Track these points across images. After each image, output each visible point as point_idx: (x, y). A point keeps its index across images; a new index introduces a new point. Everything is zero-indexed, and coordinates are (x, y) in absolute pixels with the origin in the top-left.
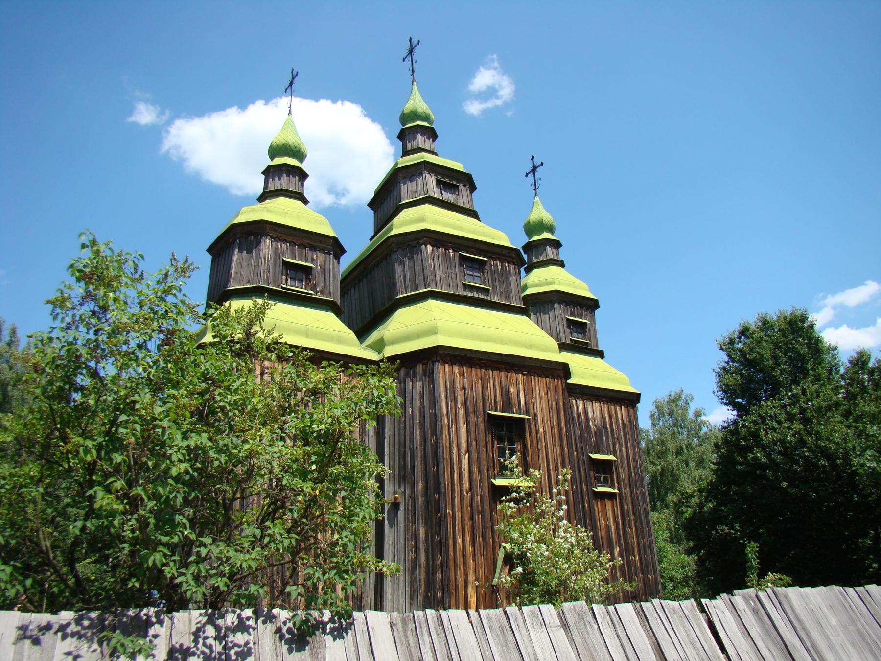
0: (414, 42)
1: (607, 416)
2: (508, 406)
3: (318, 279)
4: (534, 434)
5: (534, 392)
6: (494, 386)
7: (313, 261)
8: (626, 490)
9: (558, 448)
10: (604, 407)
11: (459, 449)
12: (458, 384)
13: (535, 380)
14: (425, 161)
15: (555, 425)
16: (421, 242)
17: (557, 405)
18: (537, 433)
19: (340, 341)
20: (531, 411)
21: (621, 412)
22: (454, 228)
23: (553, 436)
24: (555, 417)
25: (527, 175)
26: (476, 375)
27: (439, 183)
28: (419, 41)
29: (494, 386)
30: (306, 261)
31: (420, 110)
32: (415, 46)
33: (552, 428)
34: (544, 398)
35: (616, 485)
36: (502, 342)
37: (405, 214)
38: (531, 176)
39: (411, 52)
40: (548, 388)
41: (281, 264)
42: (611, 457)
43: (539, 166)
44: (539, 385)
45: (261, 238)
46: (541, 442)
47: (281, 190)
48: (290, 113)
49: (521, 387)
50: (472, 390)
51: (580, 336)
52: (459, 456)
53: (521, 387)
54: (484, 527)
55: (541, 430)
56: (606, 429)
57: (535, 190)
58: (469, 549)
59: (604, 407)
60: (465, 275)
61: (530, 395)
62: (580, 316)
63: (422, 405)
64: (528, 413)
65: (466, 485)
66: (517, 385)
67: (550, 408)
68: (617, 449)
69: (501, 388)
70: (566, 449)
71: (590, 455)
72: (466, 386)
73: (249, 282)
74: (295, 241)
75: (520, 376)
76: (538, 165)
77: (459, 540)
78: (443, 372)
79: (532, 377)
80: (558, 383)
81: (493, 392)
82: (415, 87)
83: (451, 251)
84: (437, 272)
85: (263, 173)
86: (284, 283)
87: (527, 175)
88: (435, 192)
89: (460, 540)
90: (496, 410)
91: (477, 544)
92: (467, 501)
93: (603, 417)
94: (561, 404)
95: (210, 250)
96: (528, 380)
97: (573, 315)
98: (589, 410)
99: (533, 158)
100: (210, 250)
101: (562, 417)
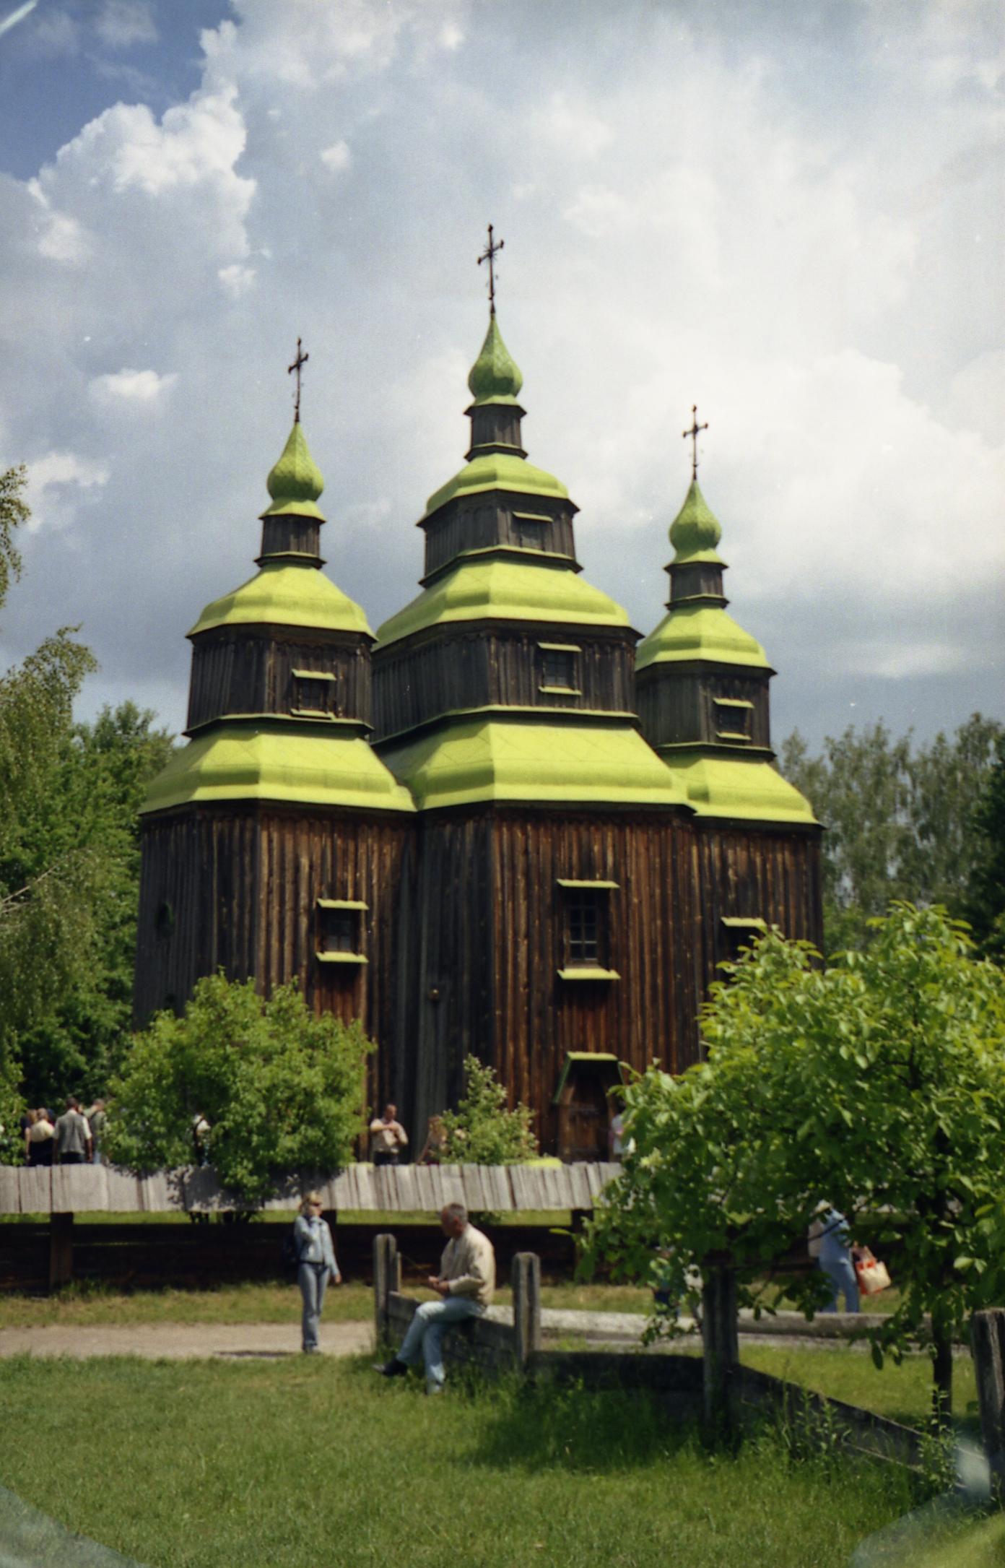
2: (586, 873)
5: (628, 847)
6: (570, 845)
7: (334, 670)
9: (659, 922)
11: (516, 934)
12: (519, 847)
15: (658, 891)
16: (482, 635)
17: (663, 864)
19: (368, 786)
20: (623, 875)
23: (652, 907)
24: (657, 881)
28: (502, 244)
29: (570, 845)
32: (497, 248)
36: (586, 781)
44: (637, 842)
48: (297, 420)
50: (538, 853)
52: (516, 944)
55: (635, 900)
58: (524, 1060)
61: (621, 853)
64: (616, 880)
65: (523, 978)
67: (650, 868)
68: (771, 909)
69: (580, 847)
70: (671, 923)
72: (530, 848)
77: (511, 1049)
83: (525, 641)
84: (502, 680)
90: (571, 878)
92: (523, 999)
93: (751, 863)
94: (669, 861)
97: (726, 695)
98: (730, 854)
101: (669, 880)
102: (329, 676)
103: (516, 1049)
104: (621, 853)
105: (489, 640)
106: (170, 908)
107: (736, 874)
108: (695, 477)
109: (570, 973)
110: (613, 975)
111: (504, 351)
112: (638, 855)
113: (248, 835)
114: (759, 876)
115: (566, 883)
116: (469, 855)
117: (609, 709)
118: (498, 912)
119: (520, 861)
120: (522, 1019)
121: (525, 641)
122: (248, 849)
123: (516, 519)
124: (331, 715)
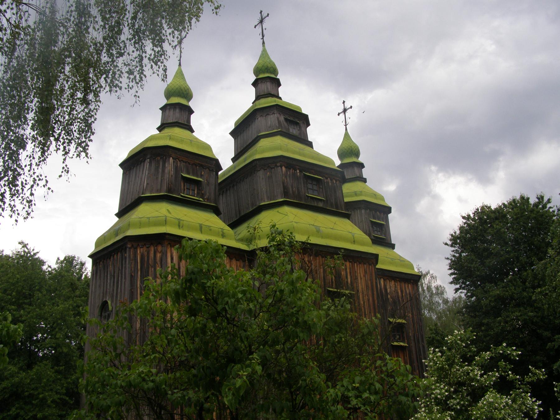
0: (264, 14)
1: (399, 291)
7: (201, 176)
8: (413, 344)
10: (398, 285)
13: (357, 266)
16: (278, 164)
18: (359, 303)
21: (408, 288)
22: (300, 154)
23: (369, 306)
24: (370, 293)
25: (339, 114)
26: (319, 262)
27: (286, 120)
30: (197, 177)
32: (265, 18)
33: (369, 300)
34: (363, 279)
35: (406, 340)
37: (263, 143)
38: (342, 115)
39: (261, 21)
40: (366, 272)
41: (180, 178)
42: (404, 321)
43: (349, 109)
45: (166, 158)
47: (176, 122)
48: (180, 65)
49: (348, 270)
51: (379, 233)
53: (348, 270)
55: (362, 302)
56: (399, 300)
57: (346, 125)
59: (398, 285)
60: (308, 189)
66: (346, 269)
67: (367, 286)
71: (389, 319)
73: (157, 192)
74: (189, 161)
75: (348, 264)
76: (348, 107)
79: (356, 264)
80: (372, 269)
83: (298, 171)
85: (161, 109)
86: (182, 192)
87: (339, 114)
90: (332, 288)
94: (374, 283)
95: (122, 165)
96: (352, 266)
98: (388, 287)
99: (344, 102)
100: (122, 165)
101: (375, 293)
104: (355, 278)
105: (281, 167)
106: (109, 302)
107: (392, 297)
108: (346, 129)
111: (269, 58)
112: (361, 278)
113: (159, 255)
114: (400, 299)
122: (159, 263)
124: (201, 199)
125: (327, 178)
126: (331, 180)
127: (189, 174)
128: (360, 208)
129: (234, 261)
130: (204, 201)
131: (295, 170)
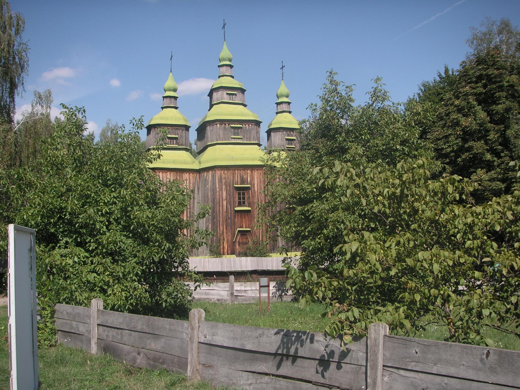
3: (180, 141)
4: (253, 191)
7: (178, 134)
11: (222, 199)
14: (221, 86)
19: (186, 163)
22: (229, 115)
27: (227, 94)
30: (176, 135)
31: (225, 57)
39: (224, 27)
40: (260, 174)
44: (256, 174)
46: (256, 193)
54: (231, 224)
55: (256, 189)
58: (225, 230)
62: (292, 136)
63: (211, 186)
64: (251, 184)
72: (226, 177)
75: (249, 171)
77: (221, 228)
78: (218, 173)
81: (237, 178)
82: (225, 43)
83: (227, 125)
88: (226, 99)
89: (221, 228)
91: (228, 229)
97: (288, 136)
102: (177, 136)
103: (223, 228)
109: (237, 209)
110: (250, 209)
112: (257, 178)
115: (235, 186)
116: (210, 179)
117: (250, 141)
118: (218, 193)
119: (223, 181)
120: (224, 221)
121: (227, 125)
123: (227, 94)
124: (177, 146)
125: (245, 125)
126: (249, 125)
127: (171, 134)
128: (279, 131)
129: (191, 174)
130: (179, 146)
131: (225, 125)
